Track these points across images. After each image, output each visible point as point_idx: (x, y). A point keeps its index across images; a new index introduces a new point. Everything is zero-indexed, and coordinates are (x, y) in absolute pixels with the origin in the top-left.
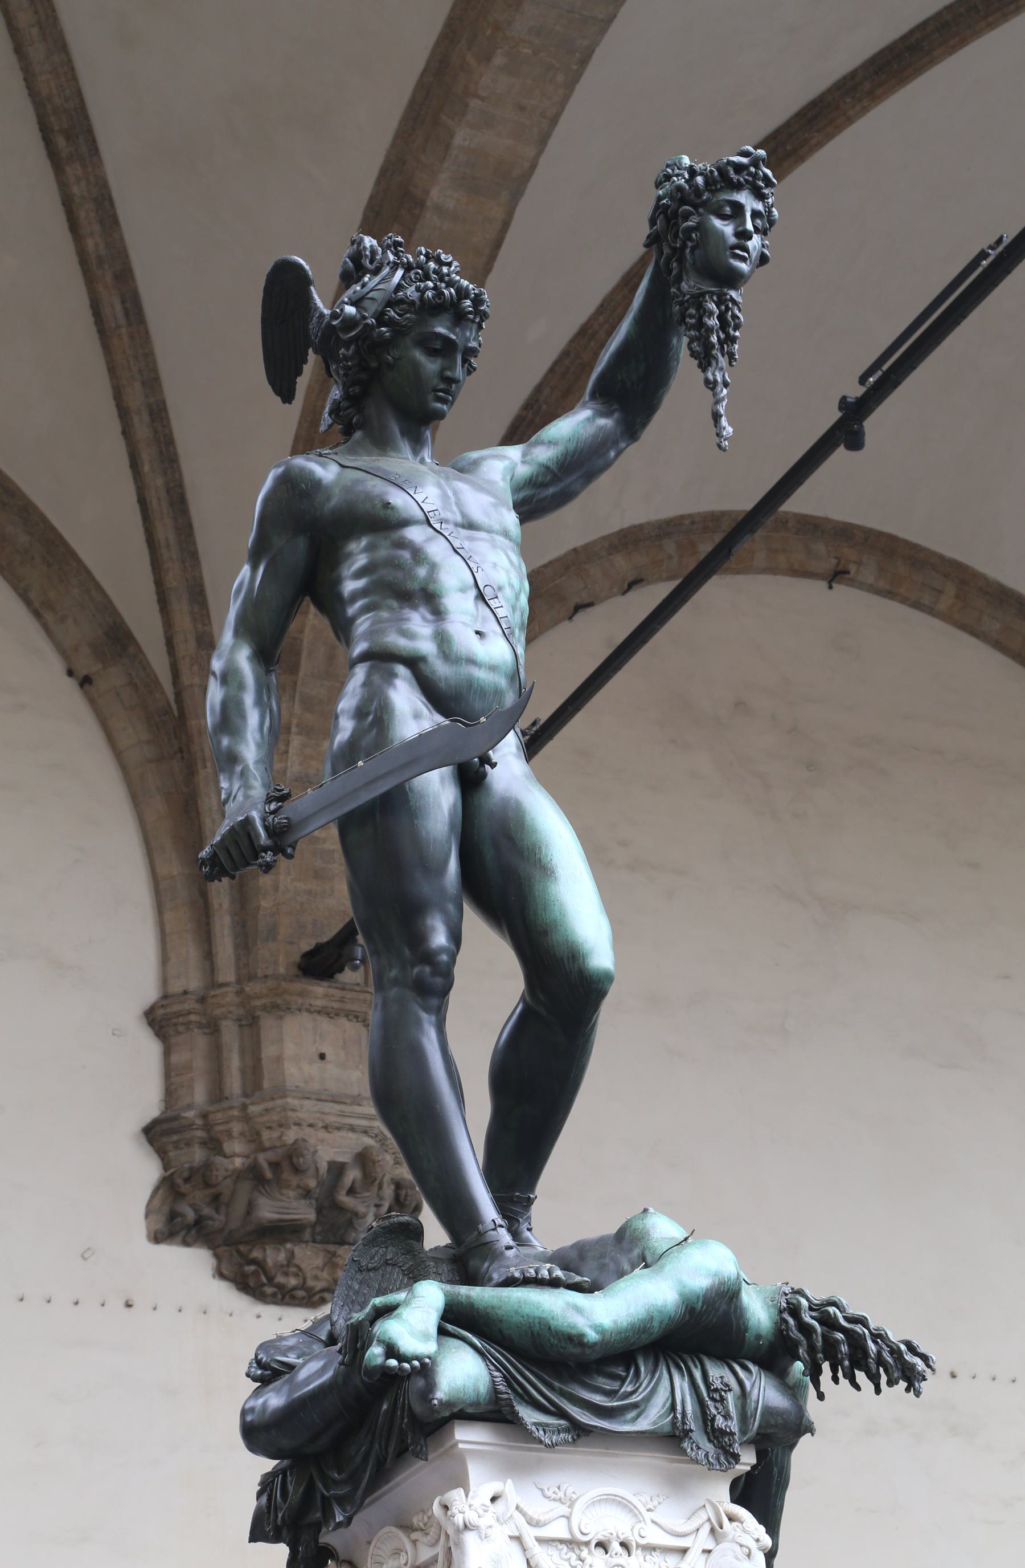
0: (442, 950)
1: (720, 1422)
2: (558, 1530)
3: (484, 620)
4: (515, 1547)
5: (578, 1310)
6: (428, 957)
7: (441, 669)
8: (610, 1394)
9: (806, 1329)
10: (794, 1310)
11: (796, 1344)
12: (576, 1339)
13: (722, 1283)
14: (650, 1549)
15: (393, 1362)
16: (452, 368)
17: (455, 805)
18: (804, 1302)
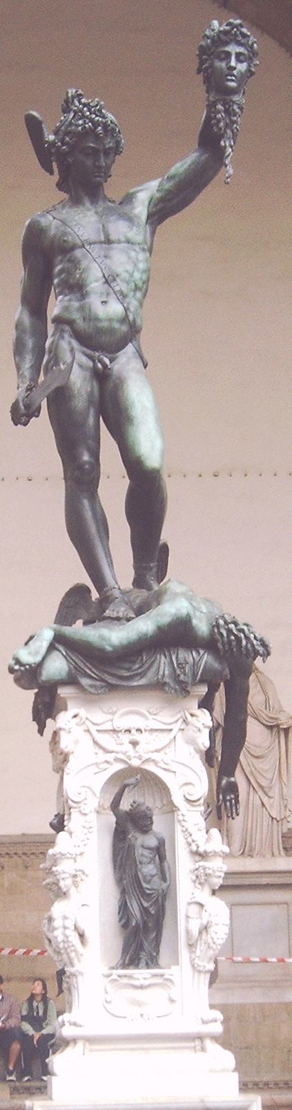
0: (86, 462)
1: (182, 677)
2: (108, 726)
3: (108, 294)
4: (87, 735)
5: (102, 638)
6: (80, 467)
7: (81, 324)
8: (129, 670)
9: (221, 635)
10: (218, 626)
11: (217, 641)
12: (102, 650)
13: (178, 619)
14: (152, 730)
15: (17, 667)
16: (98, 160)
17: (92, 391)
18: (221, 622)
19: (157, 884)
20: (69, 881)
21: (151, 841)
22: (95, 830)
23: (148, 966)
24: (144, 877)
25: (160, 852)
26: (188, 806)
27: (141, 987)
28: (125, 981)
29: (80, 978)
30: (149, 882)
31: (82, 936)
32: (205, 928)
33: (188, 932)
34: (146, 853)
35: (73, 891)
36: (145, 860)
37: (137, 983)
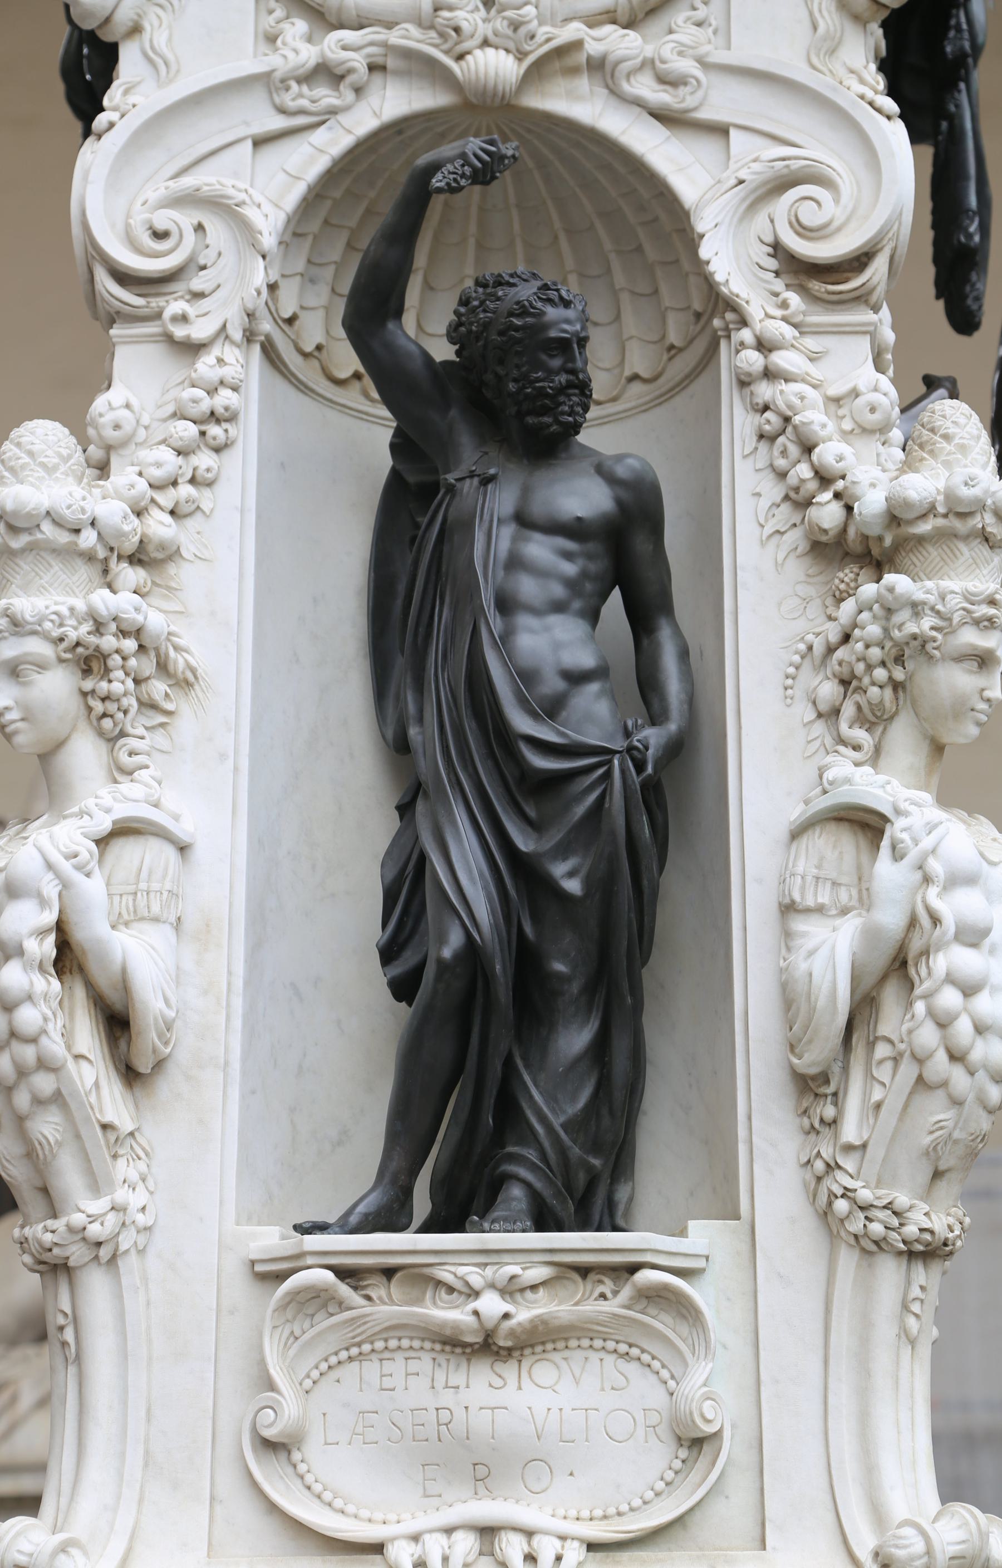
19: (594, 717)
20: (56, 687)
21: (582, 497)
22: (248, 434)
23: (544, 1220)
24: (526, 677)
25: (630, 559)
26: (794, 299)
27: (487, 1346)
28: (387, 1306)
29: (96, 1285)
30: (551, 709)
31: (116, 1022)
32: (897, 965)
33: (790, 999)
34: (540, 549)
35: (84, 754)
36: (527, 588)
37: (453, 1314)
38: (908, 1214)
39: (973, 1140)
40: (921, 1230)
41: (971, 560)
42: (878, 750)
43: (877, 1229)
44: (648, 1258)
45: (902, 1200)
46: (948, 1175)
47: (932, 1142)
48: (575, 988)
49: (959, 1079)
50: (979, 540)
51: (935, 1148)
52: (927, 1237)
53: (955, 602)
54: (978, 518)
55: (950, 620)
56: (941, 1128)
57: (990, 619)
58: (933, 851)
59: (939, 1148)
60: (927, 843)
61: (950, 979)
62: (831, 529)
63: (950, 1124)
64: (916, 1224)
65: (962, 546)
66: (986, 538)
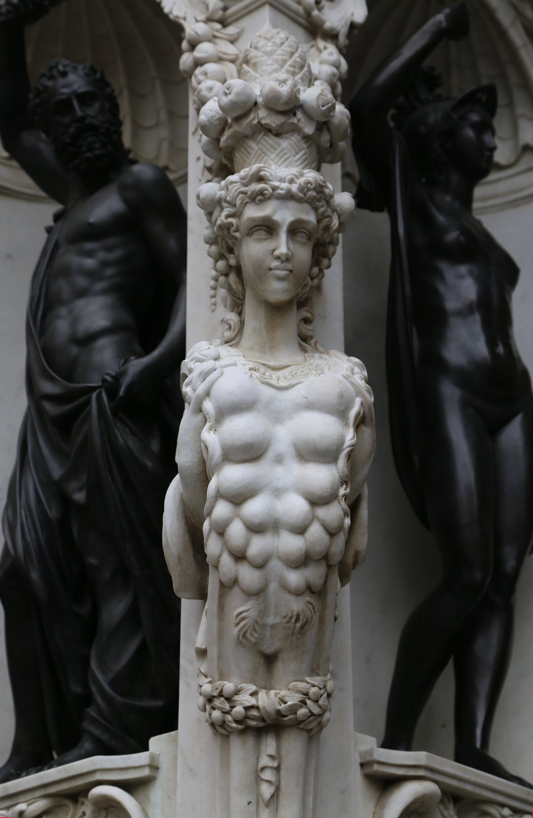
38: (236, 698)
39: (288, 622)
40: (247, 708)
41: (260, 152)
42: (242, 323)
43: (216, 714)
44: (99, 777)
45: (229, 686)
46: (281, 656)
47: (239, 631)
48: (107, 574)
49: (248, 576)
50: (263, 133)
51: (244, 635)
52: (254, 713)
53: (235, 189)
54: (252, 116)
55: (234, 206)
56: (243, 619)
57: (261, 193)
58: (207, 394)
59: (248, 635)
60: (202, 388)
61: (220, 495)
62: (212, 165)
63: (253, 614)
64: (241, 704)
65: (252, 144)
66: (268, 130)
